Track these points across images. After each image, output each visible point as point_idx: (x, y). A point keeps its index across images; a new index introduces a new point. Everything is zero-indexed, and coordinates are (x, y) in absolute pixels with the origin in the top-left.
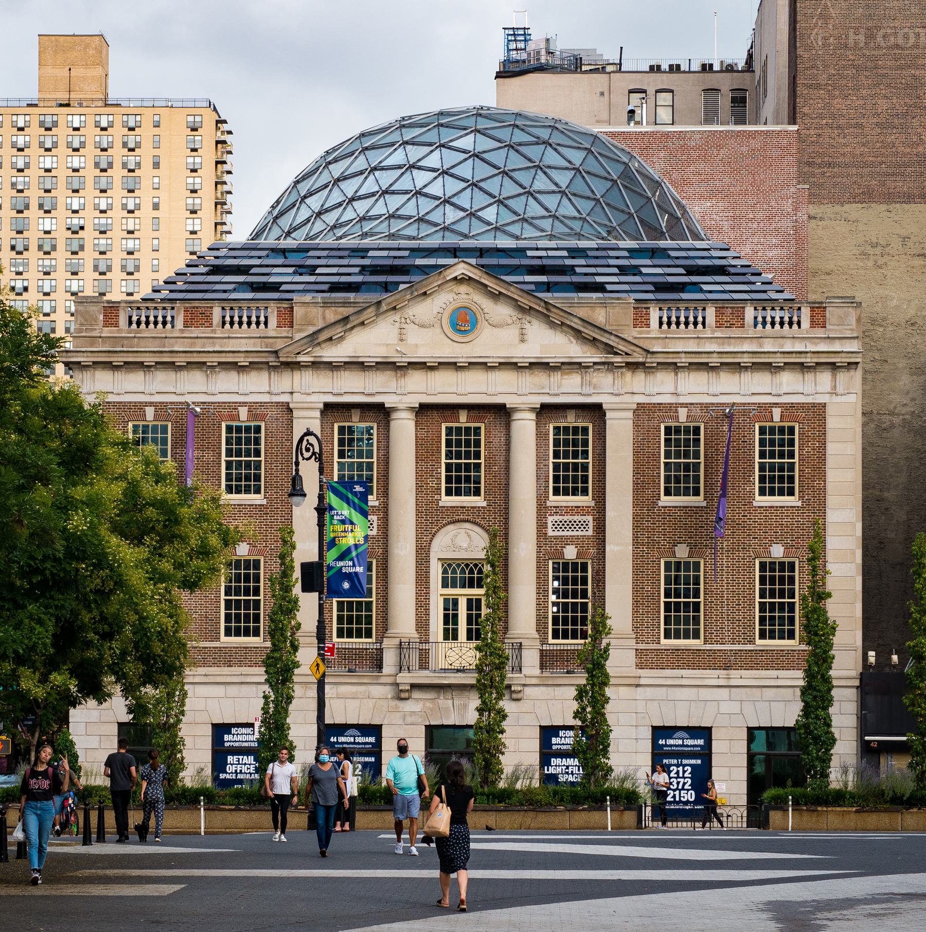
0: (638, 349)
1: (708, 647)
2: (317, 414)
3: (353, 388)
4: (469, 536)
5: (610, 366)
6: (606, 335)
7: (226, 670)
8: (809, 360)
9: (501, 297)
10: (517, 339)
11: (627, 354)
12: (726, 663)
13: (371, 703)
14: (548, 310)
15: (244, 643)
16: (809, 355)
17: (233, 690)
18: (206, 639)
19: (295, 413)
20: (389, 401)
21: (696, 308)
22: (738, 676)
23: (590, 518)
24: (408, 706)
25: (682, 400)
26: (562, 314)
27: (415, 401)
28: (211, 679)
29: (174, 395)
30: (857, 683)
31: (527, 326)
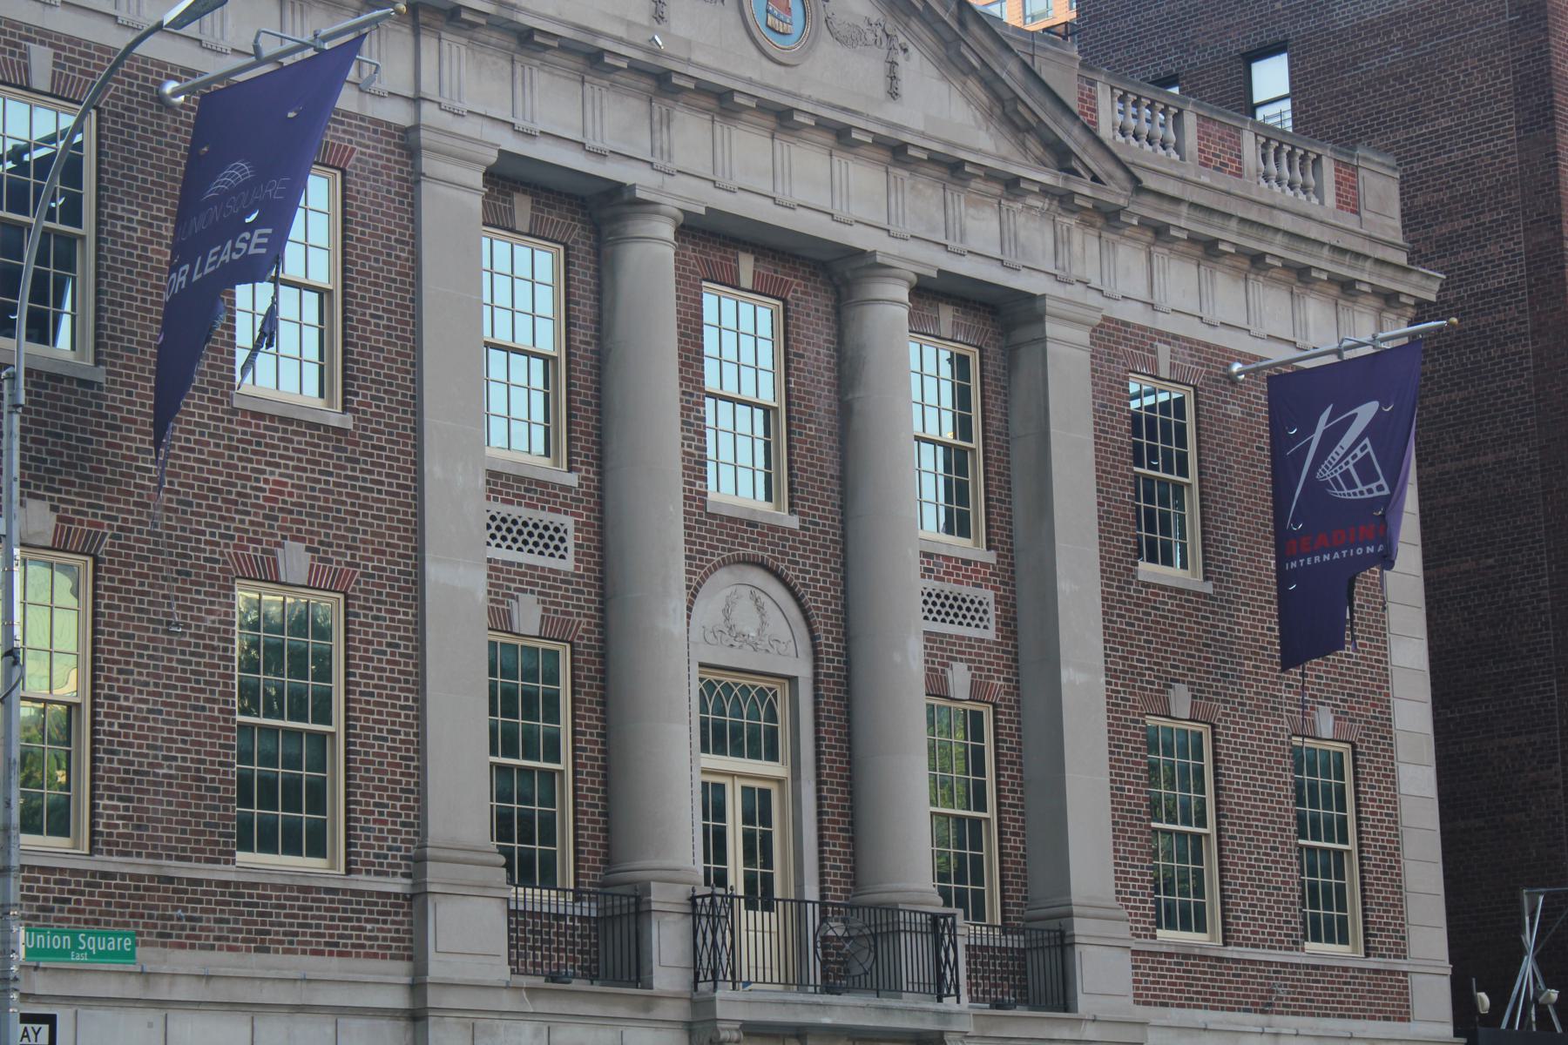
0: (1119, 174)
1: (1232, 952)
2: (476, 178)
4: (760, 608)
5: (1065, 200)
6: (1066, 121)
7: (254, 963)
8: (1365, 278)
10: (880, 88)
11: (1095, 179)
12: (1263, 994)
14: (962, 24)
15: (306, 875)
16: (1368, 265)
18: (198, 855)
19: (428, 164)
21: (1153, 102)
23: (989, 595)
25: (1166, 323)
26: (988, 42)
28: (220, 992)
29: (109, 26)
31: (900, 58)
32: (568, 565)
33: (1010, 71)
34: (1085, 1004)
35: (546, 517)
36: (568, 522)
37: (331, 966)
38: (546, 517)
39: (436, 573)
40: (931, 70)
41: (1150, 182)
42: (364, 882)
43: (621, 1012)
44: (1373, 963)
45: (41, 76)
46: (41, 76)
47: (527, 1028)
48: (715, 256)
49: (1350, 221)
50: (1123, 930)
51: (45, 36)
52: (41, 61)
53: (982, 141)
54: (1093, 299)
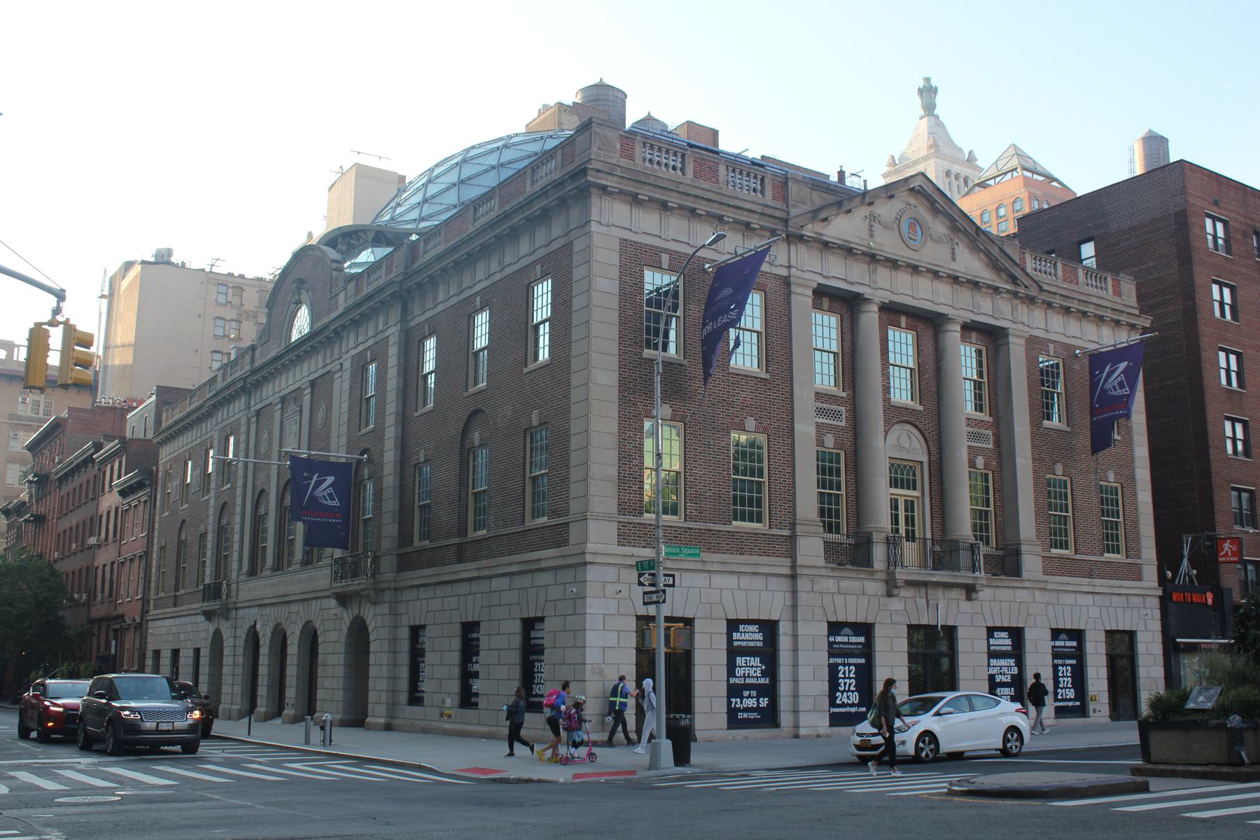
1: (1078, 557)
3: (840, 274)
5: (1015, 294)
7: (739, 558)
9: (940, 216)
10: (949, 257)
12: (1089, 571)
13: (864, 600)
17: (746, 582)
19: (793, 288)
20: (866, 291)
22: (1100, 584)
23: (990, 433)
24: (896, 604)
27: (886, 297)
28: (728, 568)
30: (1160, 593)
32: (843, 424)
33: (995, 251)
34: (1025, 574)
35: (835, 407)
36: (843, 409)
37: (765, 560)
38: (835, 407)
39: (797, 426)
40: (967, 251)
41: (1045, 287)
42: (775, 532)
43: (863, 576)
44: (1129, 561)
45: (665, 265)
46: (665, 265)
47: (831, 581)
48: (892, 317)
49: (1118, 300)
50: (1039, 549)
51: (666, 251)
52: (665, 259)
53: (986, 275)
54: (1026, 329)
